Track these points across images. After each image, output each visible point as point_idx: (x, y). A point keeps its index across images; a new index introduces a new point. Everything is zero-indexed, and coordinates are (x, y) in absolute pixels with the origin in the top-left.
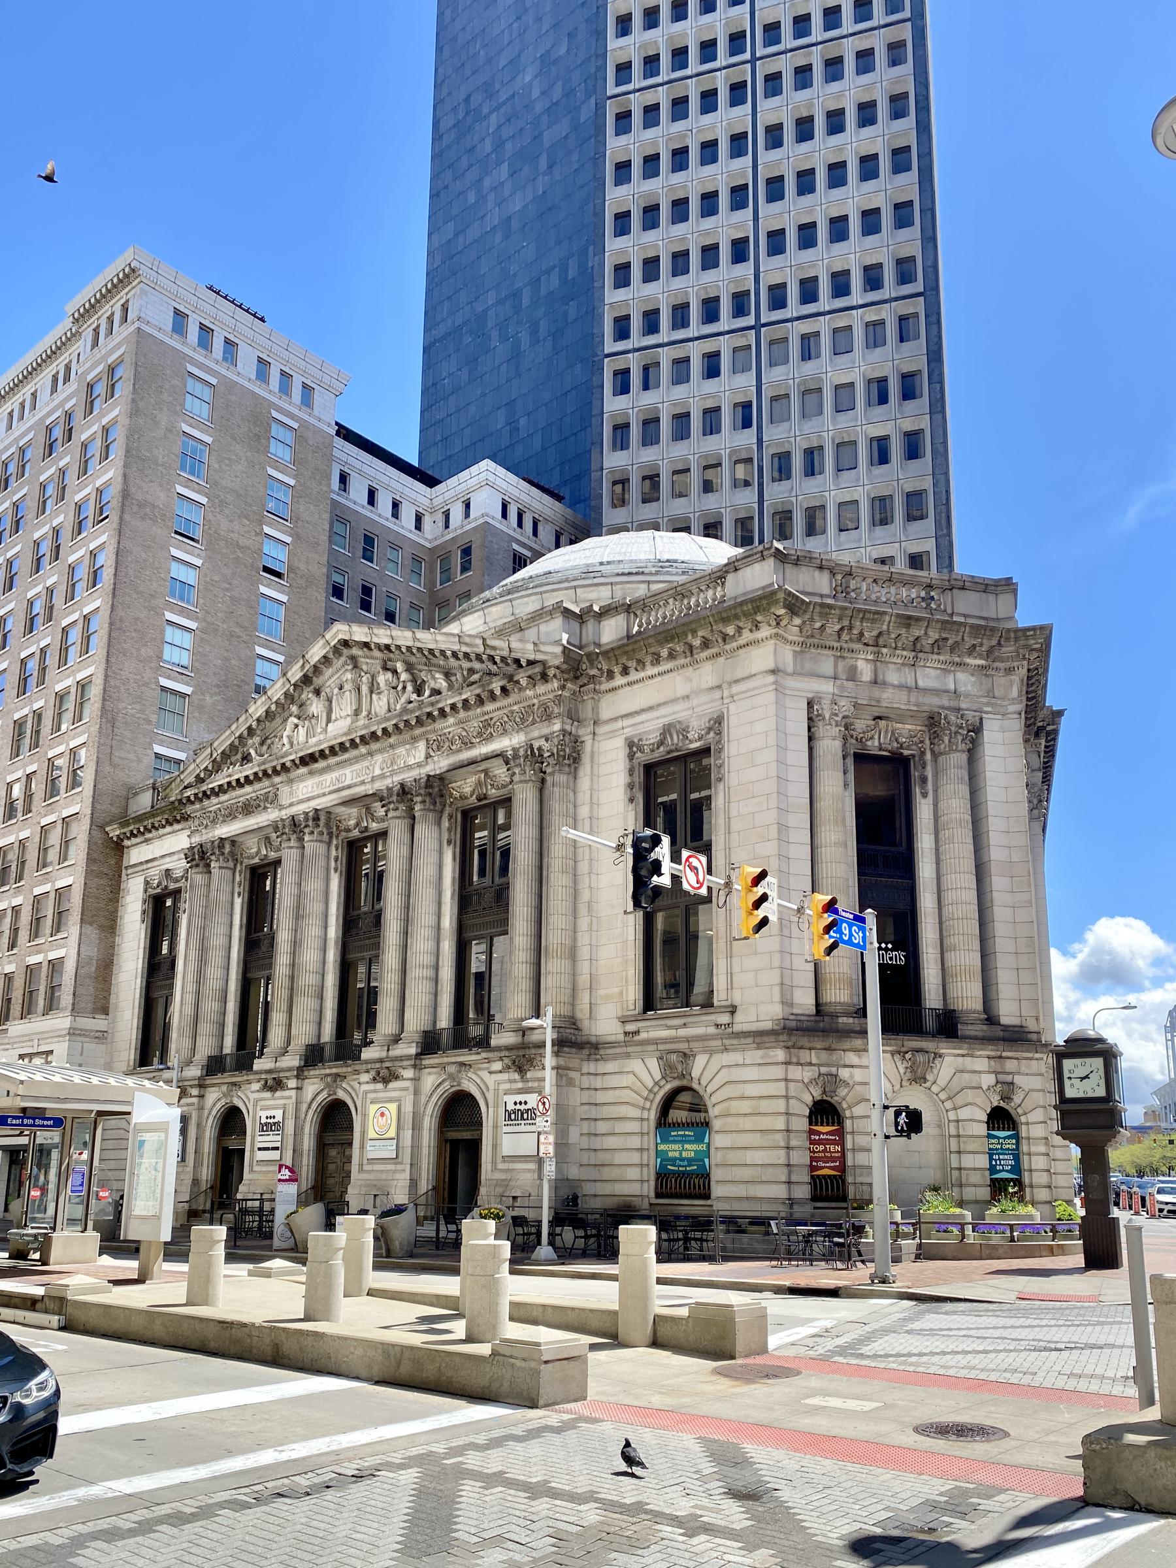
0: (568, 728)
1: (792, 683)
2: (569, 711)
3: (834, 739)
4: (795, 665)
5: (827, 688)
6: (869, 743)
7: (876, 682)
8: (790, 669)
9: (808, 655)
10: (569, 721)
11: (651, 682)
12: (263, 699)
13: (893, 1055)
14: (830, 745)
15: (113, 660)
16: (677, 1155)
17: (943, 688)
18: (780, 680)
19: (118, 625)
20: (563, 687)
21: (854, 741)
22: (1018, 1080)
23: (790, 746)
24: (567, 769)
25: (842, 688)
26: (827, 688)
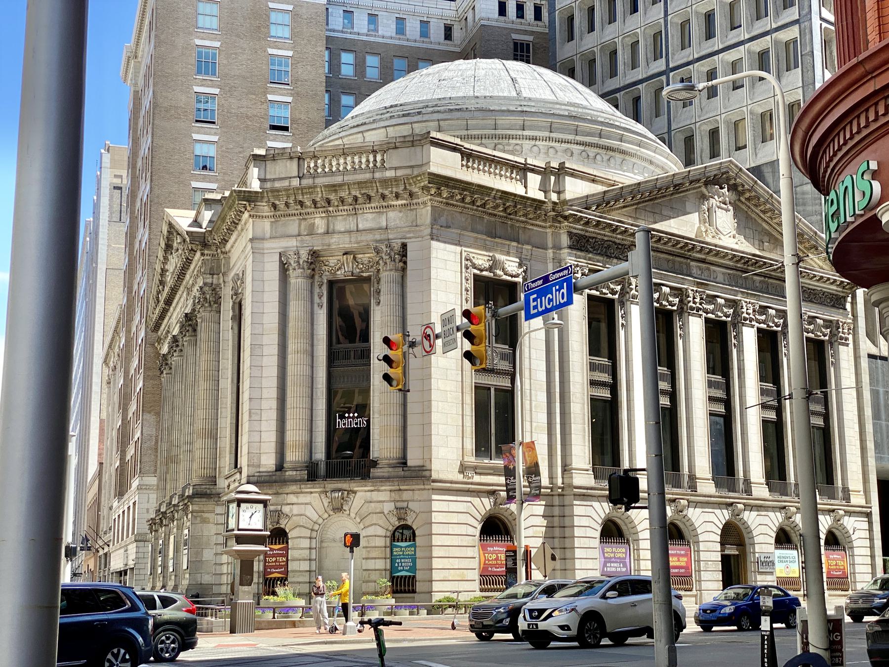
0: (209, 281)
1: (267, 244)
2: (212, 268)
3: (297, 277)
4: (271, 231)
5: (293, 243)
6: (339, 272)
7: (328, 233)
8: (268, 235)
9: (280, 223)
10: (208, 276)
11: (237, 244)
12: (158, 260)
14: (297, 280)
15: (153, 226)
16: (262, 564)
17: (377, 226)
18: (257, 245)
19: (156, 200)
20: (202, 254)
21: (328, 273)
22: (411, 505)
23: (266, 289)
24: (209, 309)
25: (302, 241)
26: (293, 243)
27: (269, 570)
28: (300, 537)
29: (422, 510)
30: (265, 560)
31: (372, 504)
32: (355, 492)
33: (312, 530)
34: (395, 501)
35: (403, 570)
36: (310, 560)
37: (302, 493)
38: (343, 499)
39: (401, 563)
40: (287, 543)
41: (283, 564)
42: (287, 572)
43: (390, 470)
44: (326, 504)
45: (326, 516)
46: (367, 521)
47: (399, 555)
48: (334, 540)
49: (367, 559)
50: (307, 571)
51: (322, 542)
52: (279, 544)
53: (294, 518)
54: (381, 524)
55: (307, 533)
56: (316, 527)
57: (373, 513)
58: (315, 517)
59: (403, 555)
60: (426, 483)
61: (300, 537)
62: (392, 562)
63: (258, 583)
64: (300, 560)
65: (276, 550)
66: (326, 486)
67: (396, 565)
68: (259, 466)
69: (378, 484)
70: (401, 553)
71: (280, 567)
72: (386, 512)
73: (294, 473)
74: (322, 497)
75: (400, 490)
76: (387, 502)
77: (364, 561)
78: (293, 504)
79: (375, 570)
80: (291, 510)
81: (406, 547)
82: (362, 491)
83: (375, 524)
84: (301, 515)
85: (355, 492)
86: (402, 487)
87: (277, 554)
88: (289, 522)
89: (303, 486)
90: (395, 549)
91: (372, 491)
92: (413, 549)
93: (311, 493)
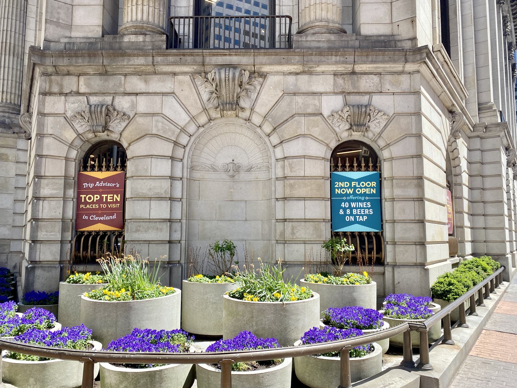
13: (193, 80)
27: (85, 217)
28: (151, 156)
29: (399, 110)
30: (79, 199)
31: (299, 99)
32: (264, 76)
33: (176, 143)
34: (344, 93)
35: (356, 222)
36: (172, 199)
37: (155, 73)
38: (240, 86)
39: (351, 209)
40: (124, 167)
41: (114, 206)
42: (122, 223)
43: (332, 37)
44: (205, 96)
45: (203, 119)
46: (288, 130)
47: (347, 195)
48: (214, 169)
49: (285, 199)
50: (164, 220)
51: (192, 168)
52: (108, 170)
53: (140, 120)
54: (316, 134)
55: (167, 149)
56: (184, 140)
57: (299, 114)
58: (182, 119)
59: (354, 194)
60: (410, 58)
61: (151, 156)
62: (334, 206)
63: (62, 242)
64: (150, 199)
65: (100, 180)
66: (208, 59)
67: (341, 212)
68: (70, 27)
69: (315, 58)
70: (351, 191)
71: (109, 212)
72: (326, 113)
73: (141, 38)
74: (198, 83)
75: (353, 73)
76: (326, 93)
77: (279, 204)
78: (137, 94)
79: (305, 220)
80: (134, 106)
81: (359, 180)
82: (277, 73)
83: (304, 136)
84: (153, 115)
85: (264, 76)
86: (359, 68)
87: (102, 187)
88: (130, 128)
89: (159, 59)
90: (338, 184)
91: (297, 74)
92: (374, 184)
93: (175, 74)
